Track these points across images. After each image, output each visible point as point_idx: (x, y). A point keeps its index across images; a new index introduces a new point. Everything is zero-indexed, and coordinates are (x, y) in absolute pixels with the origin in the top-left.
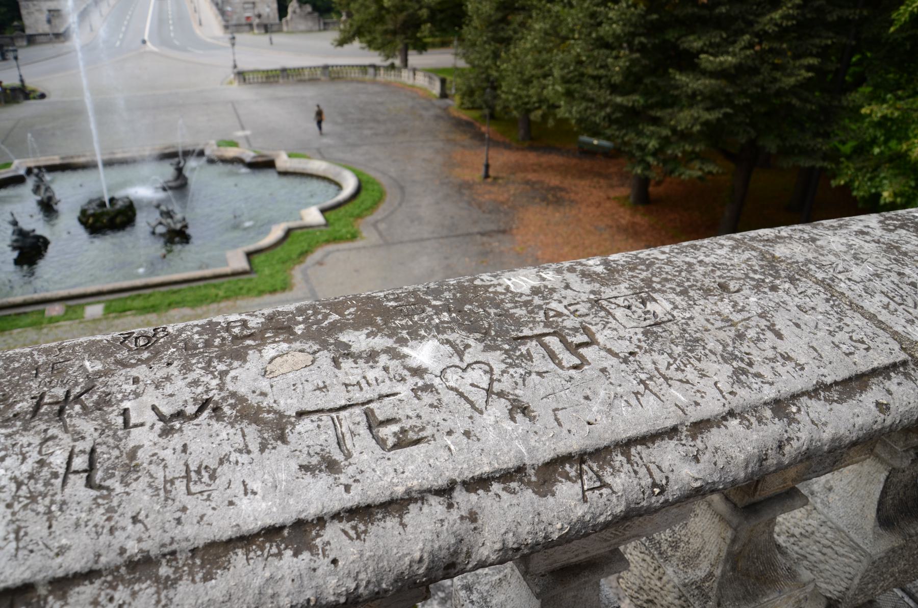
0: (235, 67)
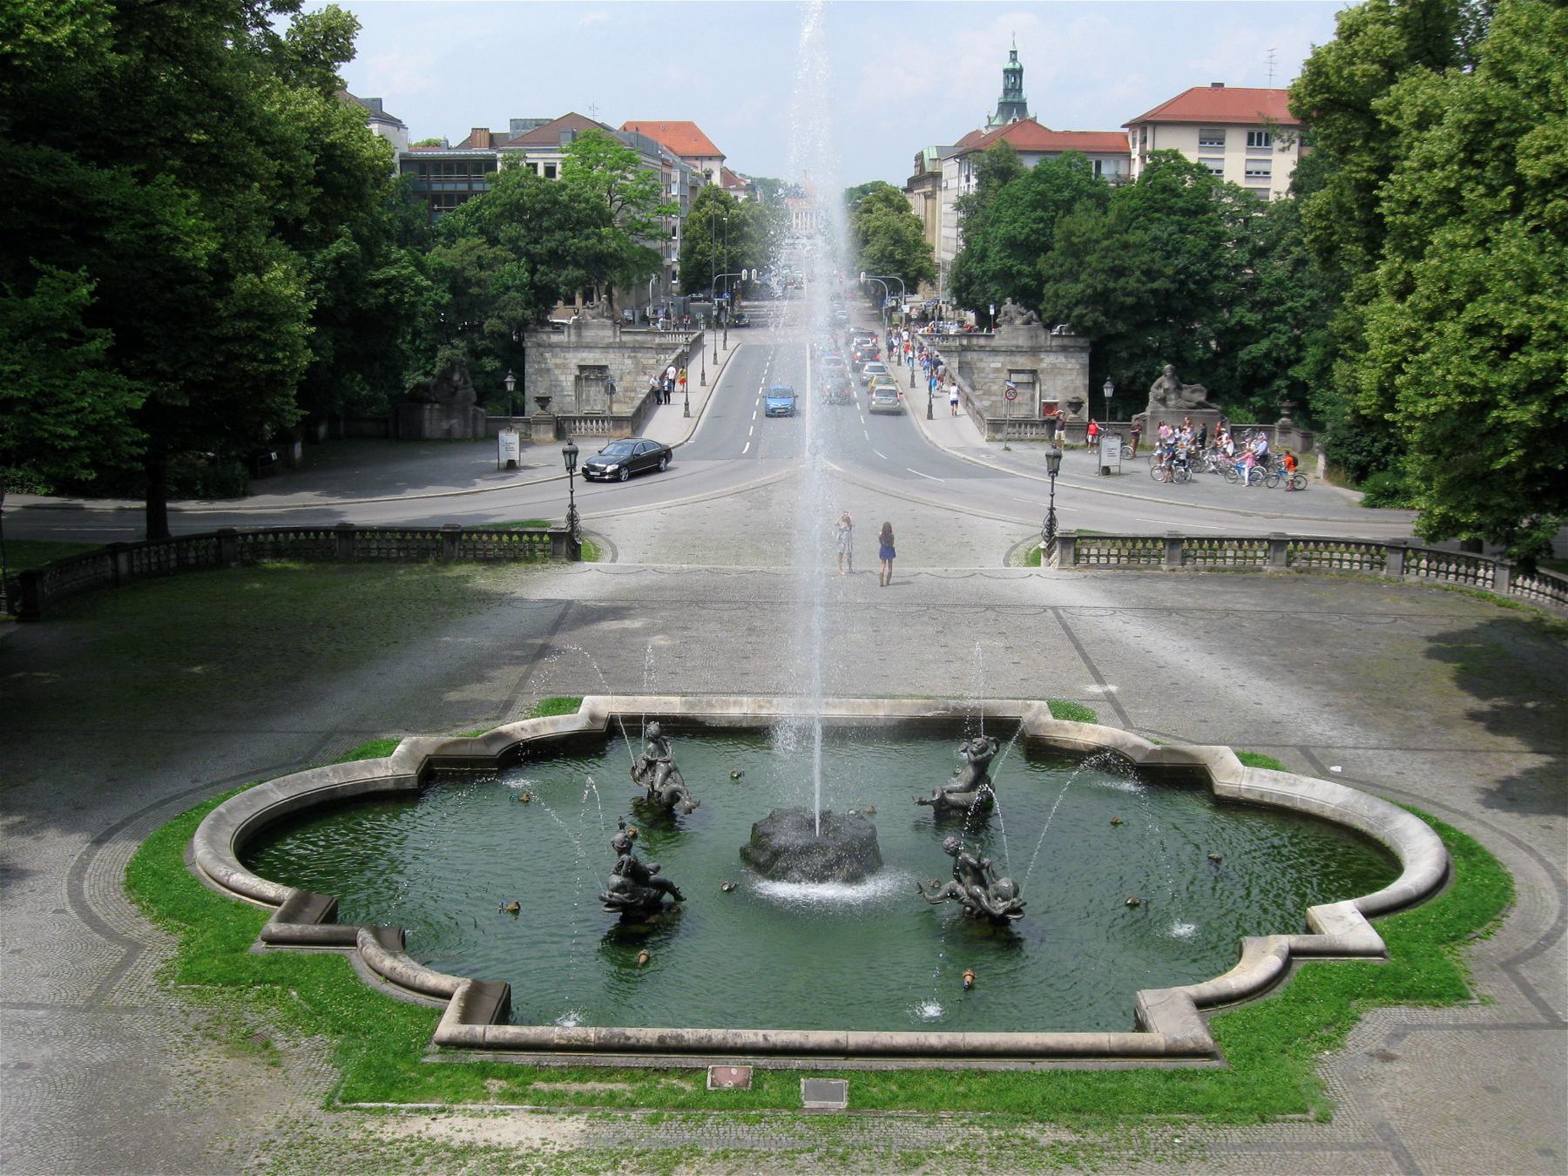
0: (1052, 522)
